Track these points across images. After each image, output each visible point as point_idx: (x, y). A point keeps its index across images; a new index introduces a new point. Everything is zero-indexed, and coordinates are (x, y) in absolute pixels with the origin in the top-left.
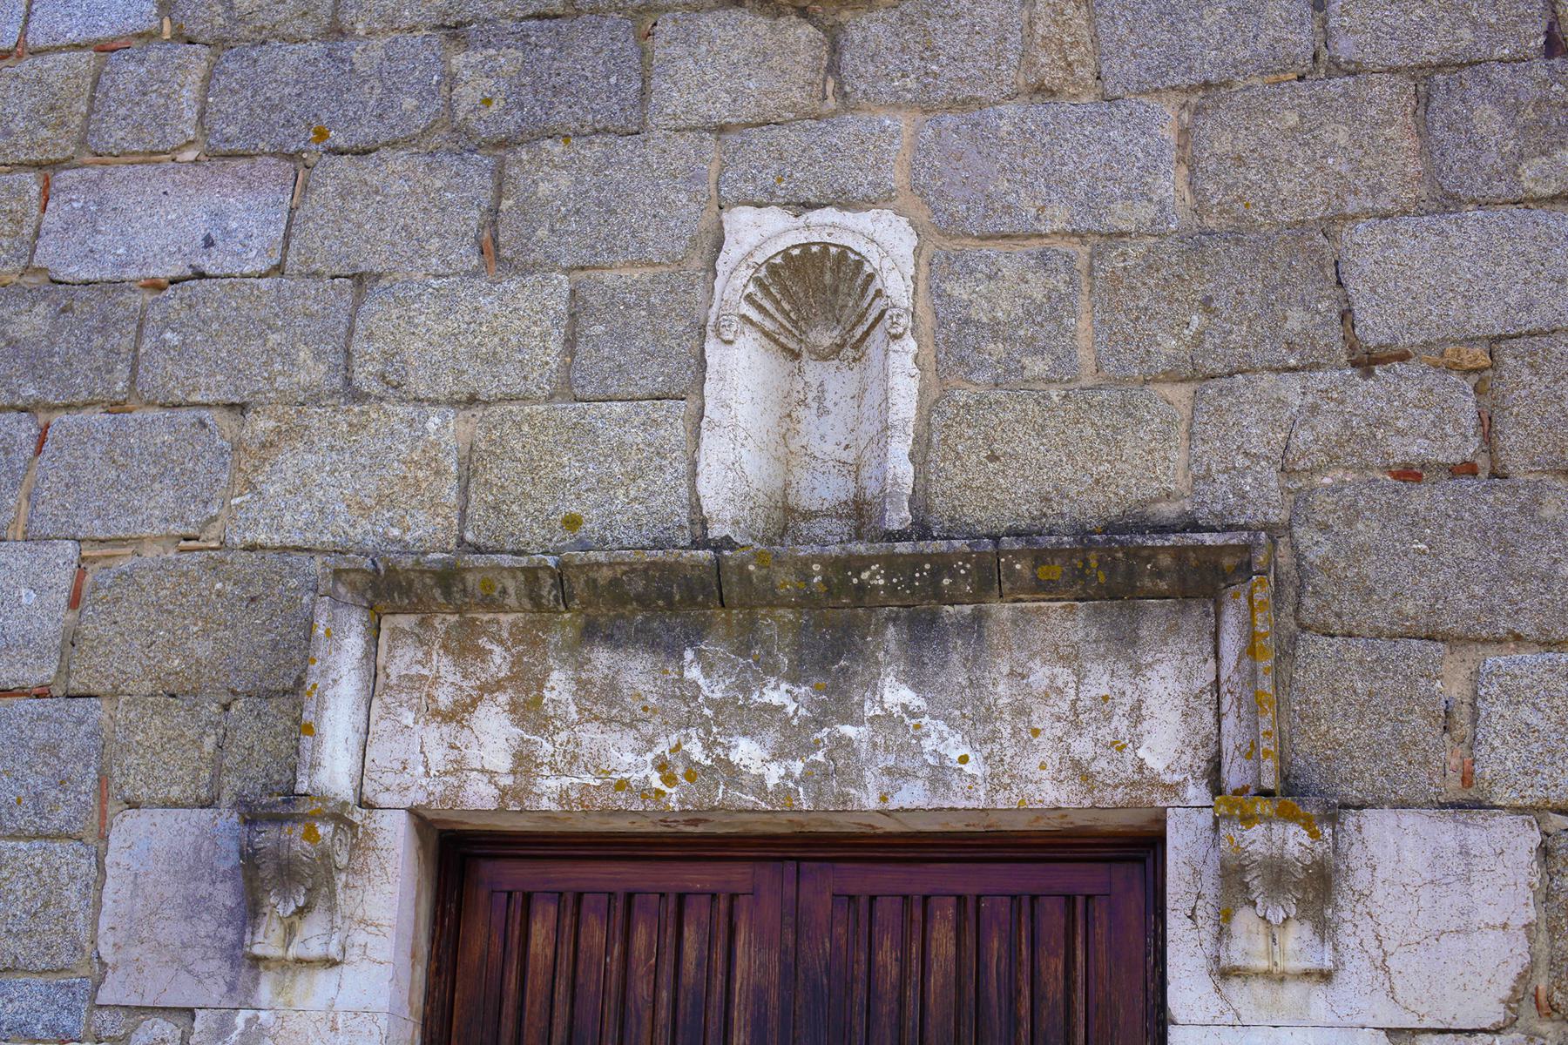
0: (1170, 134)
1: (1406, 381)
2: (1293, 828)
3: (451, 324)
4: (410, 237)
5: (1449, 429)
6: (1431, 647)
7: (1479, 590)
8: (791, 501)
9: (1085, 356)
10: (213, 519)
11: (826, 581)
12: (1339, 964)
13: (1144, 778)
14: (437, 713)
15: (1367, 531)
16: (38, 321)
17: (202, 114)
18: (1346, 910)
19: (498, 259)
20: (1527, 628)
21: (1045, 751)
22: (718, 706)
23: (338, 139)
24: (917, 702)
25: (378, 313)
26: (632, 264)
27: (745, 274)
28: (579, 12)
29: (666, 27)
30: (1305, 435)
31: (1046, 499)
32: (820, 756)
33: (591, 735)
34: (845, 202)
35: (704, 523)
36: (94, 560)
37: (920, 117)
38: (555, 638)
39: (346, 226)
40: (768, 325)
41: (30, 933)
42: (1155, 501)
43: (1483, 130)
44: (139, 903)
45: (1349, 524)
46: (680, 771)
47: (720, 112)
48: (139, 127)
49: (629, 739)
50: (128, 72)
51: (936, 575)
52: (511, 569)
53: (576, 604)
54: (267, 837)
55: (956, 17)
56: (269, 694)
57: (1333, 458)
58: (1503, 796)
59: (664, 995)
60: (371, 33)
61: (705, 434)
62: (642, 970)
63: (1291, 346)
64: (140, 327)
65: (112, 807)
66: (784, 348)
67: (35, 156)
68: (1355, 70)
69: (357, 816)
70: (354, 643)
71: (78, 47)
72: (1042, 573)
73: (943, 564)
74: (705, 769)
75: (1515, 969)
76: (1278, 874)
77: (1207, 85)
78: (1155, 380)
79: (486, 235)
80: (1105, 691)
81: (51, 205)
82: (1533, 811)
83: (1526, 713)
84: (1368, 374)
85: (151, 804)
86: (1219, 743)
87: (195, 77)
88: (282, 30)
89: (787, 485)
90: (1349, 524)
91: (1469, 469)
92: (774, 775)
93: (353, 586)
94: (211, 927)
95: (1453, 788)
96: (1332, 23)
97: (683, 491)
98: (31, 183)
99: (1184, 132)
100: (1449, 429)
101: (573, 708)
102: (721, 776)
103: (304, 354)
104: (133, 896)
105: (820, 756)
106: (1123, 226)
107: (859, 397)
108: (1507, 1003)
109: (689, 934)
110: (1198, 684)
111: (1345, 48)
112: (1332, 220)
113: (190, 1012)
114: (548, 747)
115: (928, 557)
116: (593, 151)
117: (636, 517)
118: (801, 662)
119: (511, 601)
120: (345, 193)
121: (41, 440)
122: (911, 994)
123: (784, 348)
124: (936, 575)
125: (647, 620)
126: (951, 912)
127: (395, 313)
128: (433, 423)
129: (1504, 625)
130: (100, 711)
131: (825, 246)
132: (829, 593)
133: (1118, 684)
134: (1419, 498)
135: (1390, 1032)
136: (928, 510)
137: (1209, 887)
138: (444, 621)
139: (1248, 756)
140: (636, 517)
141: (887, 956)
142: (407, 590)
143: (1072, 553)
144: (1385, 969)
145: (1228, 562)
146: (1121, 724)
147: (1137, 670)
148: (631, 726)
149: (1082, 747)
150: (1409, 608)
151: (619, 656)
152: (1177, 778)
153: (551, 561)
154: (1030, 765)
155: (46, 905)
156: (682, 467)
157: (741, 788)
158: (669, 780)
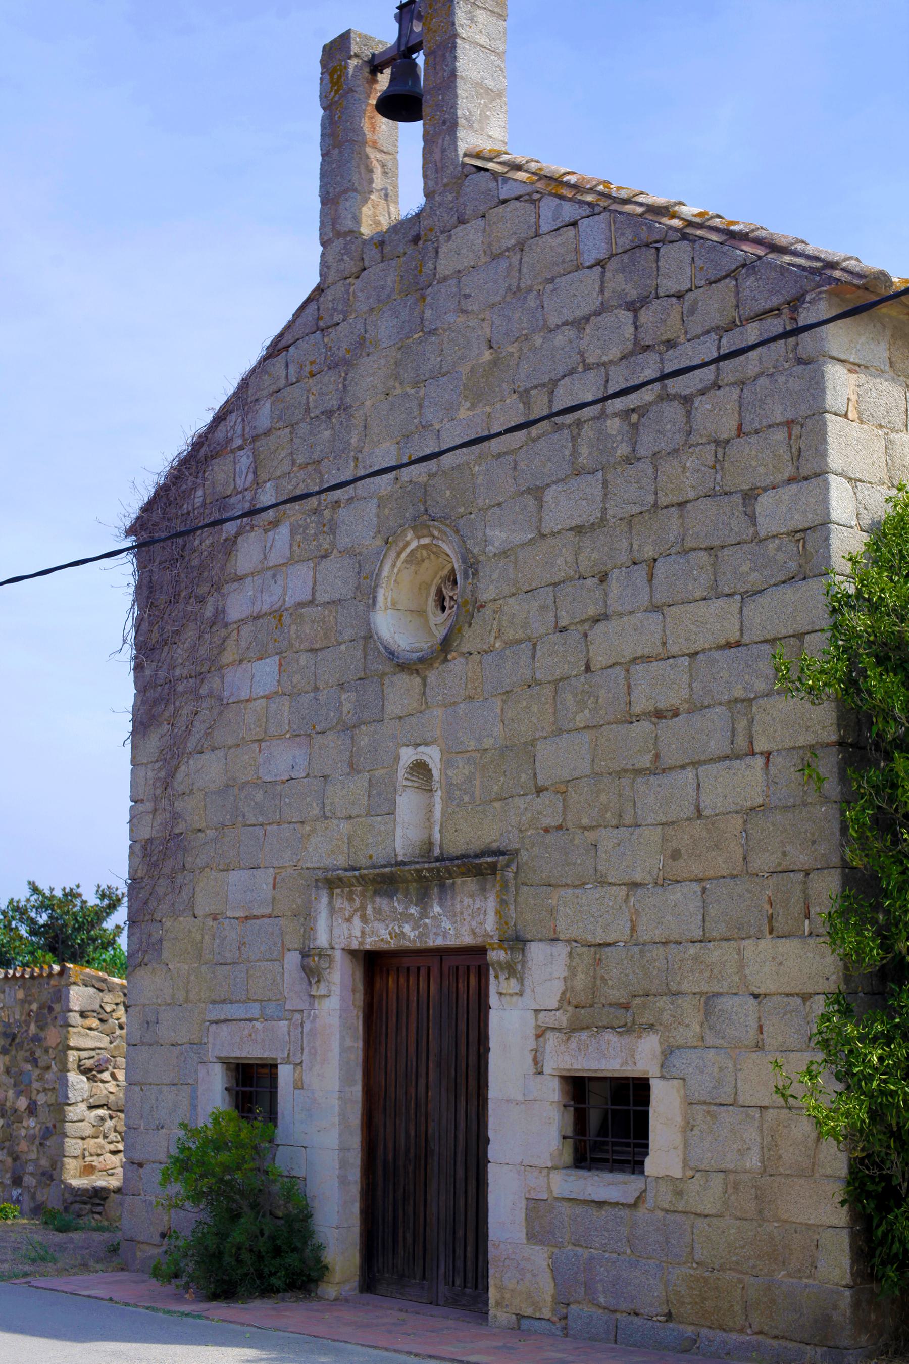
0: (498, 711)
6: (549, 888)
7: (559, 869)
13: (487, 935)
20: (569, 882)
21: (466, 927)
22: (401, 914)
29: (387, 682)
30: (524, 818)
38: (368, 894)
40: (416, 785)
58: (562, 937)
70: (325, 900)
75: (561, 991)
77: (507, 692)
82: (568, 941)
91: (560, 828)
92: (412, 935)
108: (559, 1002)
111: (539, 676)
129: (564, 880)
147: (486, 898)
149: (474, 924)
154: (463, 931)
158: (391, 938)
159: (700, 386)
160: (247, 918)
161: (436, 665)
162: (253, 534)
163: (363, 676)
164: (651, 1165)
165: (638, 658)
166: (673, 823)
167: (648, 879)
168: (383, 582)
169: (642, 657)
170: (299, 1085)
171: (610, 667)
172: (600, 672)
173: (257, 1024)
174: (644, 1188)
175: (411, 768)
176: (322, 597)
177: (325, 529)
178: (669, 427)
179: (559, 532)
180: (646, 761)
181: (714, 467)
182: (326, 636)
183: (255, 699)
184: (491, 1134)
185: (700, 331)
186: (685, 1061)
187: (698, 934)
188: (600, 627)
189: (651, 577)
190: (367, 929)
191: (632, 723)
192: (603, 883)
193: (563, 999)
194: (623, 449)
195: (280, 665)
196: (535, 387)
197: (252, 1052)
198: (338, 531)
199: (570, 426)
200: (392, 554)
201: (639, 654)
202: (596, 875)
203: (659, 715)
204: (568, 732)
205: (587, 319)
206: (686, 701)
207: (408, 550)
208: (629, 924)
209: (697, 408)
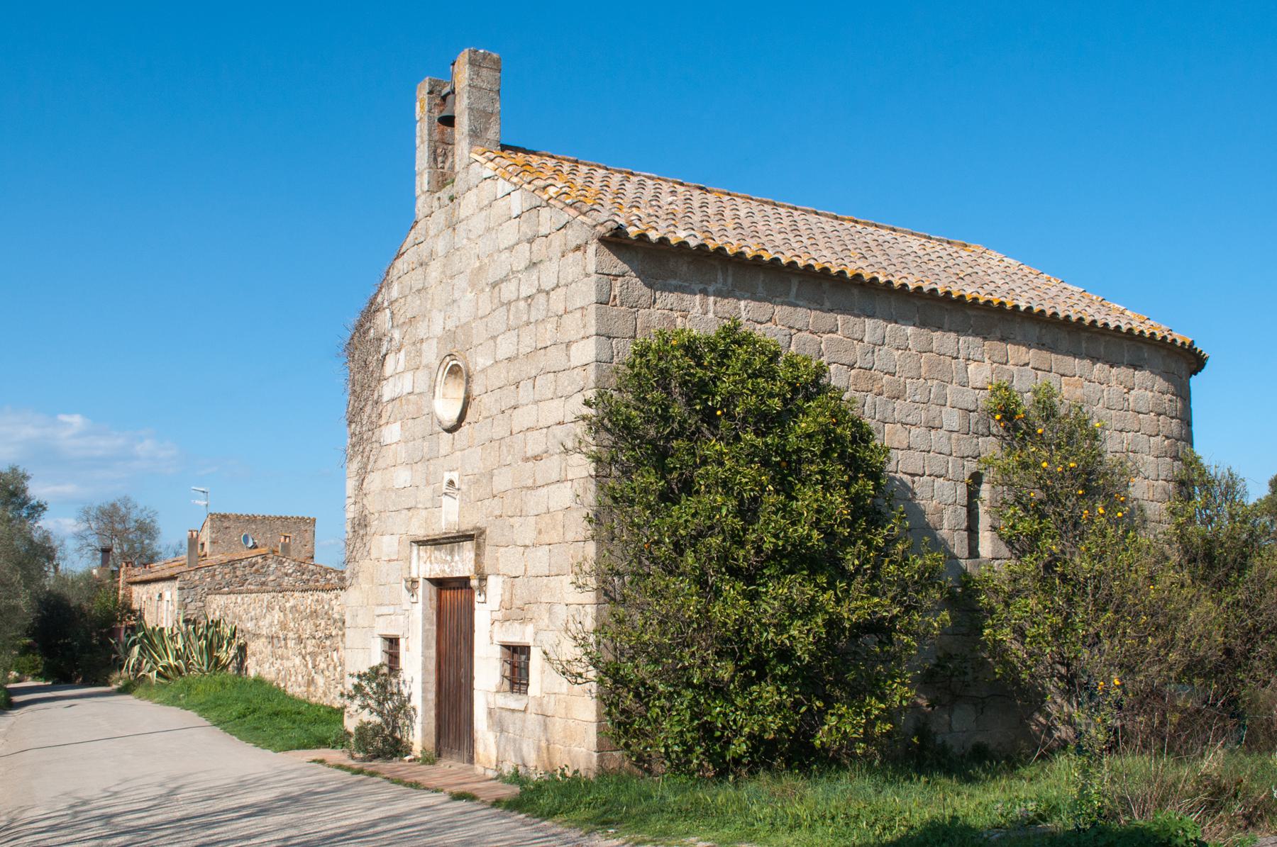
167: (531, 544)
170: (407, 649)
176: (417, 391)
180: (530, 483)
184: (476, 674)
187: (547, 574)
194: (525, 318)
197: (391, 632)
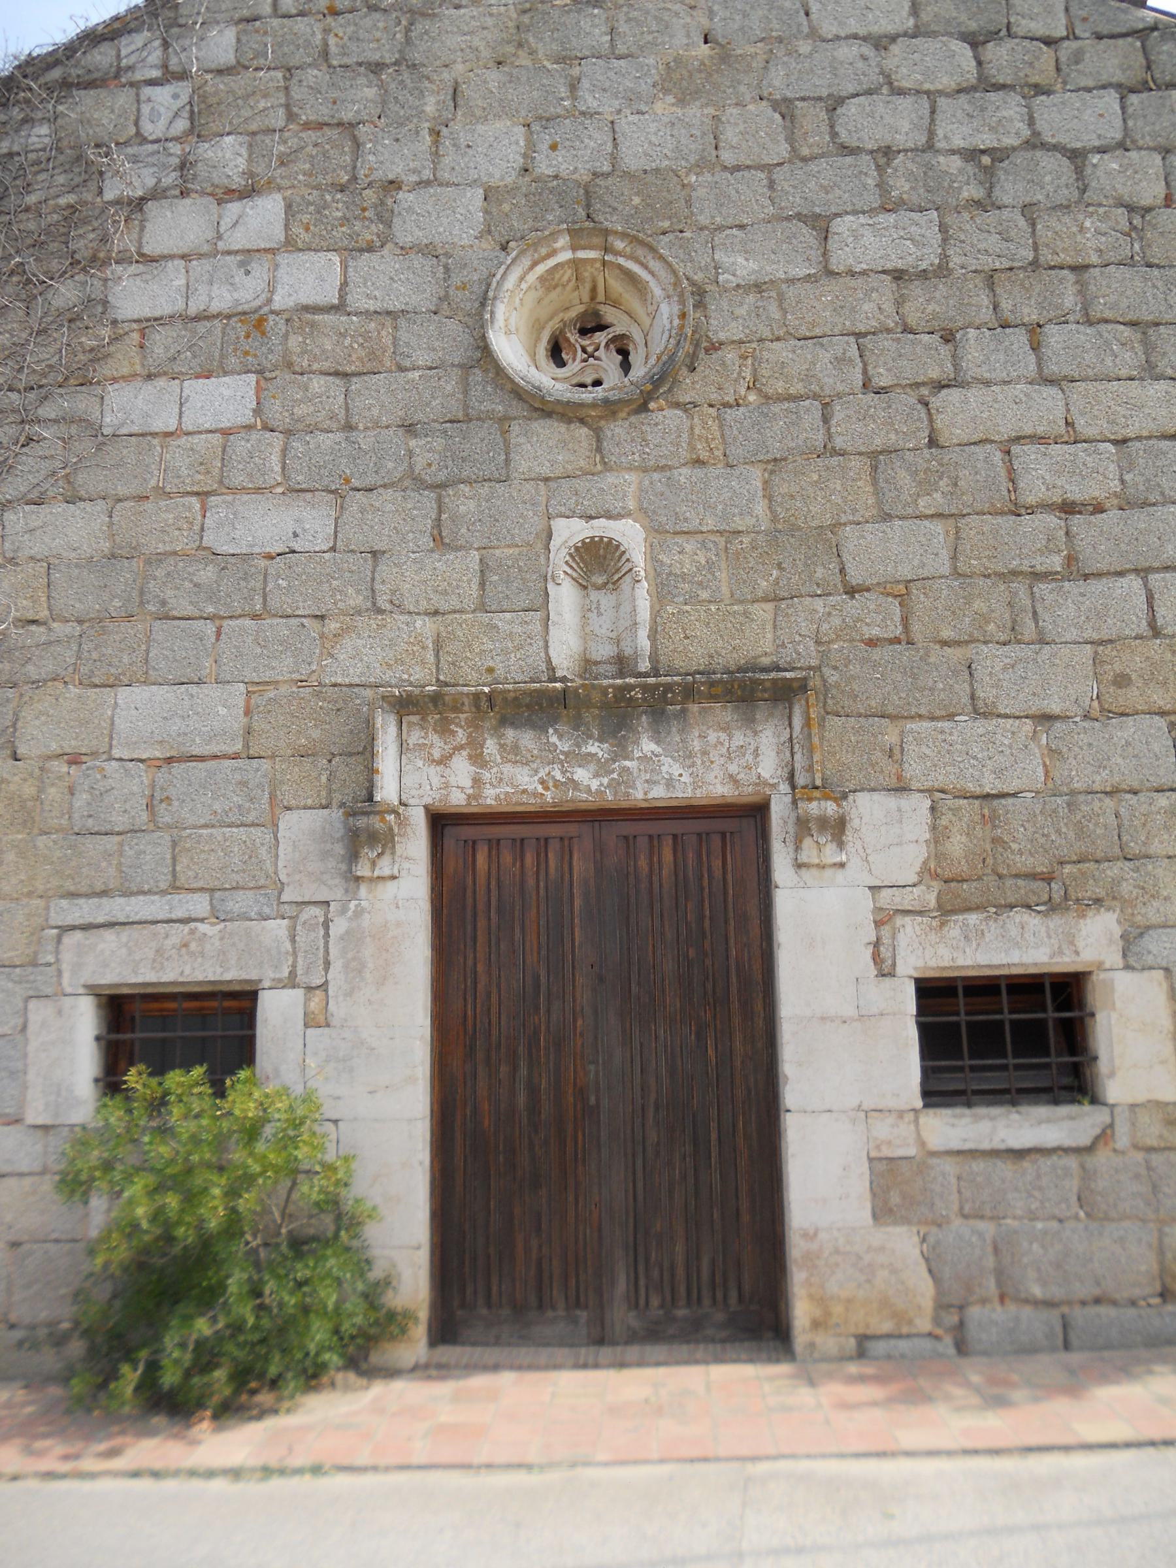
0: (759, 485)
1: (870, 600)
2: (829, 803)
3: (424, 575)
4: (398, 533)
5: (889, 622)
6: (883, 720)
7: (903, 695)
8: (588, 656)
9: (725, 590)
10: (314, 672)
11: (615, 696)
12: (848, 860)
13: (761, 782)
14: (434, 761)
15: (854, 669)
16: (209, 574)
17: (283, 468)
18: (849, 836)
19: (443, 544)
20: (923, 711)
22: (566, 754)
23: (355, 483)
24: (658, 750)
25: (385, 569)
26: (509, 546)
27: (564, 551)
28: (471, 420)
29: (515, 428)
30: (825, 626)
31: (711, 657)
32: (615, 776)
33: (508, 769)
34: (609, 516)
35: (553, 669)
36: (254, 692)
37: (642, 475)
39: (365, 527)
40: (575, 575)
41: (244, 871)
42: (760, 657)
43: (901, 483)
44: (297, 854)
45: (846, 666)
46: (551, 784)
47: (546, 471)
48: (250, 475)
49: (526, 770)
50: (241, 446)
51: (665, 692)
52: (468, 694)
53: (497, 709)
54: (362, 822)
55: (656, 424)
56: (351, 755)
57: (838, 636)
58: (915, 785)
59: (542, 884)
60: (367, 428)
61: (551, 627)
62: (530, 873)
63: (818, 585)
64: (265, 577)
65: (277, 811)
66: (581, 585)
67: (195, 489)
68: (843, 453)
69: (401, 809)
70: (392, 730)
71: (211, 432)
72: (713, 691)
73: (668, 687)
74: (562, 783)
76: (823, 823)
77: (775, 460)
78: (758, 601)
79: (435, 532)
80: (741, 743)
81: (208, 514)
82: (929, 791)
83: (924, 749)
84: (853, 597)
85: (298, 808)
86: (793, 765)
87: (278, 449)
88: (320, 426)
89: (586, 649)
90: (846, 666)
91: (896, 641)
92: (594, 785)
93: (389, 703)
94: (334, 864)
95: (894, 782)
96: (833, 430)
97: (542, 654)
98: (195, 502)
99: (766, 482)
100: (889, 622)
101: (498, 757)
102: (570, 786)
103: (350, 591)
104: (294, 851)
105: (615, 776)
106: (740, 529)
107: (617, 607)
108: (918, 874)
109: (551, 855)
110: (782, 739)
111: (839, 443)
112: (834, 526)
113: (327, 903)
114: (488, 775)
115: (660, 685)
116: (485, 490)
117: (521, 667)
118: (604, 733)
119: (466, 708)
120: (362, 511)
121: (218, 634)
122: (655, 879)
123: (581, 585)
124: (665, 692)
125: (529, 715)
126: (670, 842)
127: (394, 570)
128: (419, 623)
129: (914, 710)
130: (265, 765)
131: (602, 538)
132: (616, 702)
133: (747, 740)
134: (876, 654)
135: (870, 888)
136: (658, 662)
137: (791, 829)
138: (433, 718)
139: (807, 771)
140: (521, 667)
141: (643, 863)
142: (416, 704)
143: (727, 682)
144: (867, 862)
145: (795, 685)
146: (749, 758)
147: (756, 733)
148: (526, 764)
149: (733, 768)
150: (873, 704)
151: (518, 732)
152: (775, 781)
153: (486, 690)
154: (710, 777)
155: (250, 857)
156: (541, 643)
157: (580, 791)
158: (547, 788)
159: (1097, 143)
160: (169, 760)
161: (623, 415)
162: (188, 201)
163: (460, 416)
164: (1115, 1090)
165: (1024, 437)
166: (1111, 641)
167: (1074, 709)
168: (504, 295)
169: (1030, 437)
171: (975, 443)
172: (957, 449)
173: (202, 928)
174: (1108, 1120)
175: (577, 549)
177: (366, 214)
178: (1048, 178)
179: (864, 273)
180: (1056, 562)
181: (1129, 235)
182: (372, 355)
183: (188, 434)
185: (1091, 83)
186: (1168, 945)
188: (952, 396)
189: (1036, 347)
190: (486, 776)
191: (1019, 515)
192: (981, 711)
193: (928, 873)
194: (973, 191)
195: (259, 390)
196: (803, 99)
198: (397, 221)
199: (872, 152)
200: (526, 262)
201: (1028, 431)
202: (974, 706)
203: (1068, 508)
204: (902, 518)
205: (893, 39)
206: (1115, 494)
207: (551, 263)
208: (1040, 771)
209: (1095, 166)
